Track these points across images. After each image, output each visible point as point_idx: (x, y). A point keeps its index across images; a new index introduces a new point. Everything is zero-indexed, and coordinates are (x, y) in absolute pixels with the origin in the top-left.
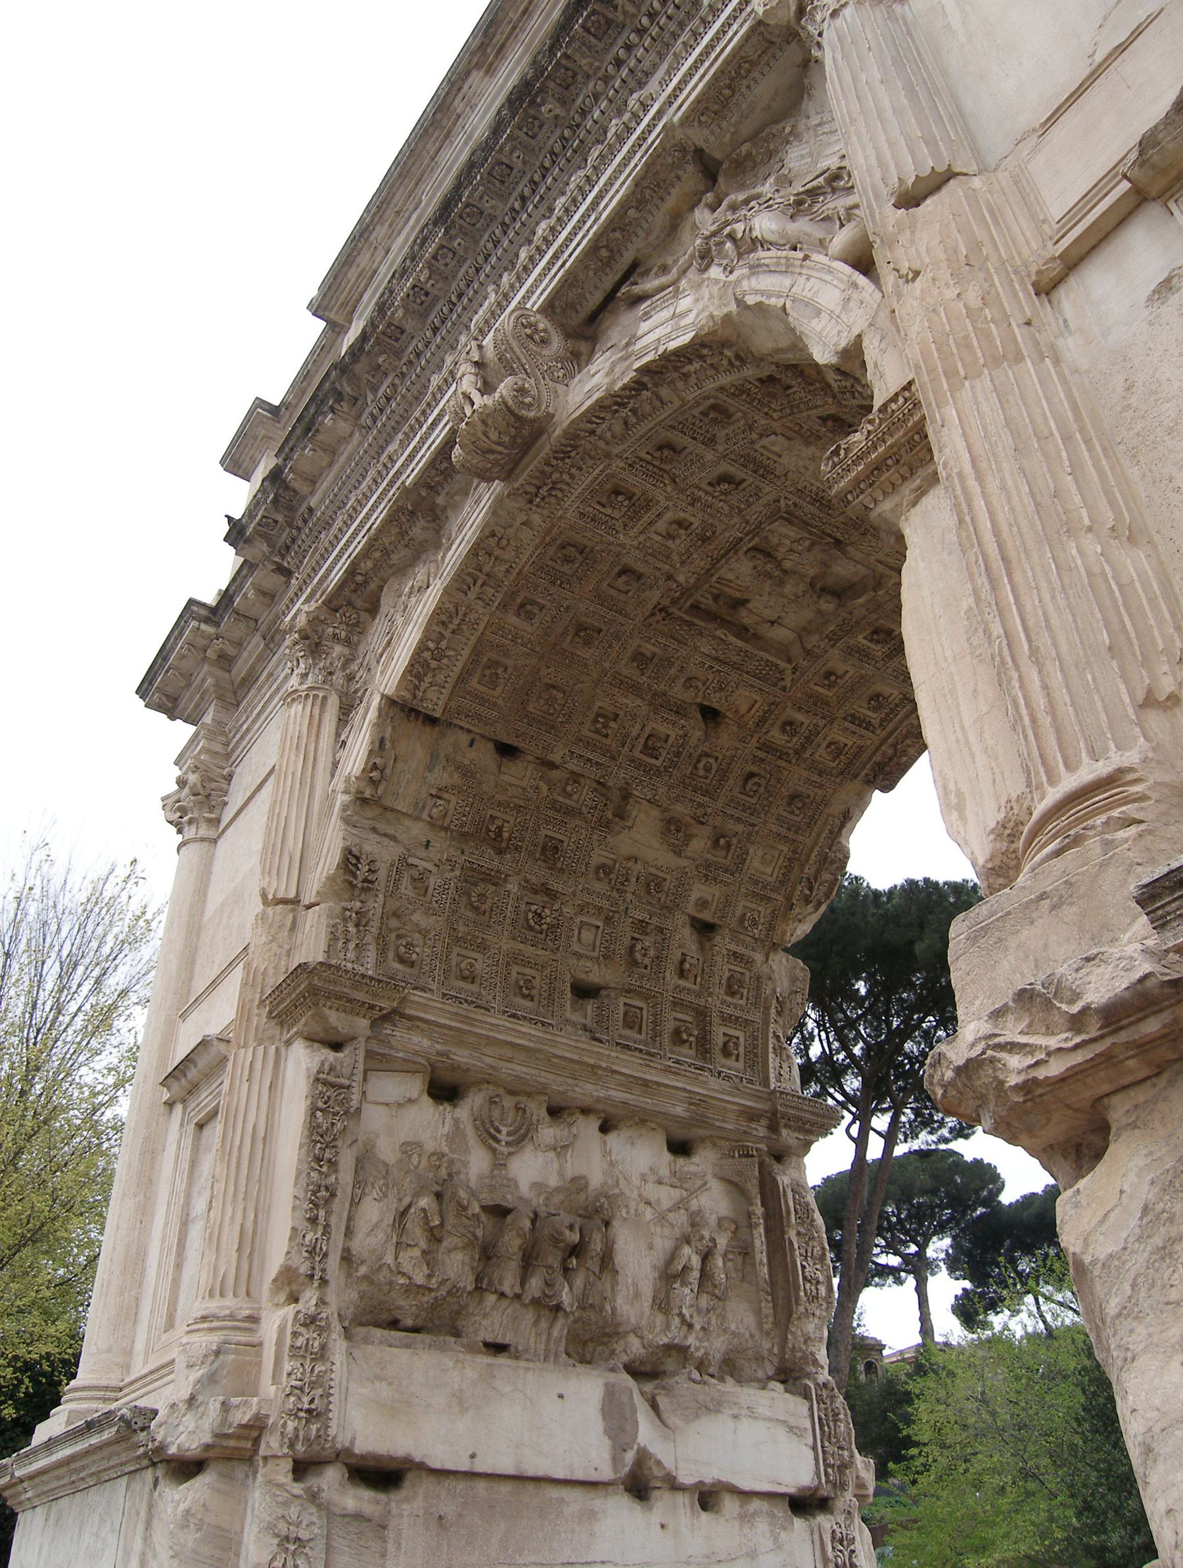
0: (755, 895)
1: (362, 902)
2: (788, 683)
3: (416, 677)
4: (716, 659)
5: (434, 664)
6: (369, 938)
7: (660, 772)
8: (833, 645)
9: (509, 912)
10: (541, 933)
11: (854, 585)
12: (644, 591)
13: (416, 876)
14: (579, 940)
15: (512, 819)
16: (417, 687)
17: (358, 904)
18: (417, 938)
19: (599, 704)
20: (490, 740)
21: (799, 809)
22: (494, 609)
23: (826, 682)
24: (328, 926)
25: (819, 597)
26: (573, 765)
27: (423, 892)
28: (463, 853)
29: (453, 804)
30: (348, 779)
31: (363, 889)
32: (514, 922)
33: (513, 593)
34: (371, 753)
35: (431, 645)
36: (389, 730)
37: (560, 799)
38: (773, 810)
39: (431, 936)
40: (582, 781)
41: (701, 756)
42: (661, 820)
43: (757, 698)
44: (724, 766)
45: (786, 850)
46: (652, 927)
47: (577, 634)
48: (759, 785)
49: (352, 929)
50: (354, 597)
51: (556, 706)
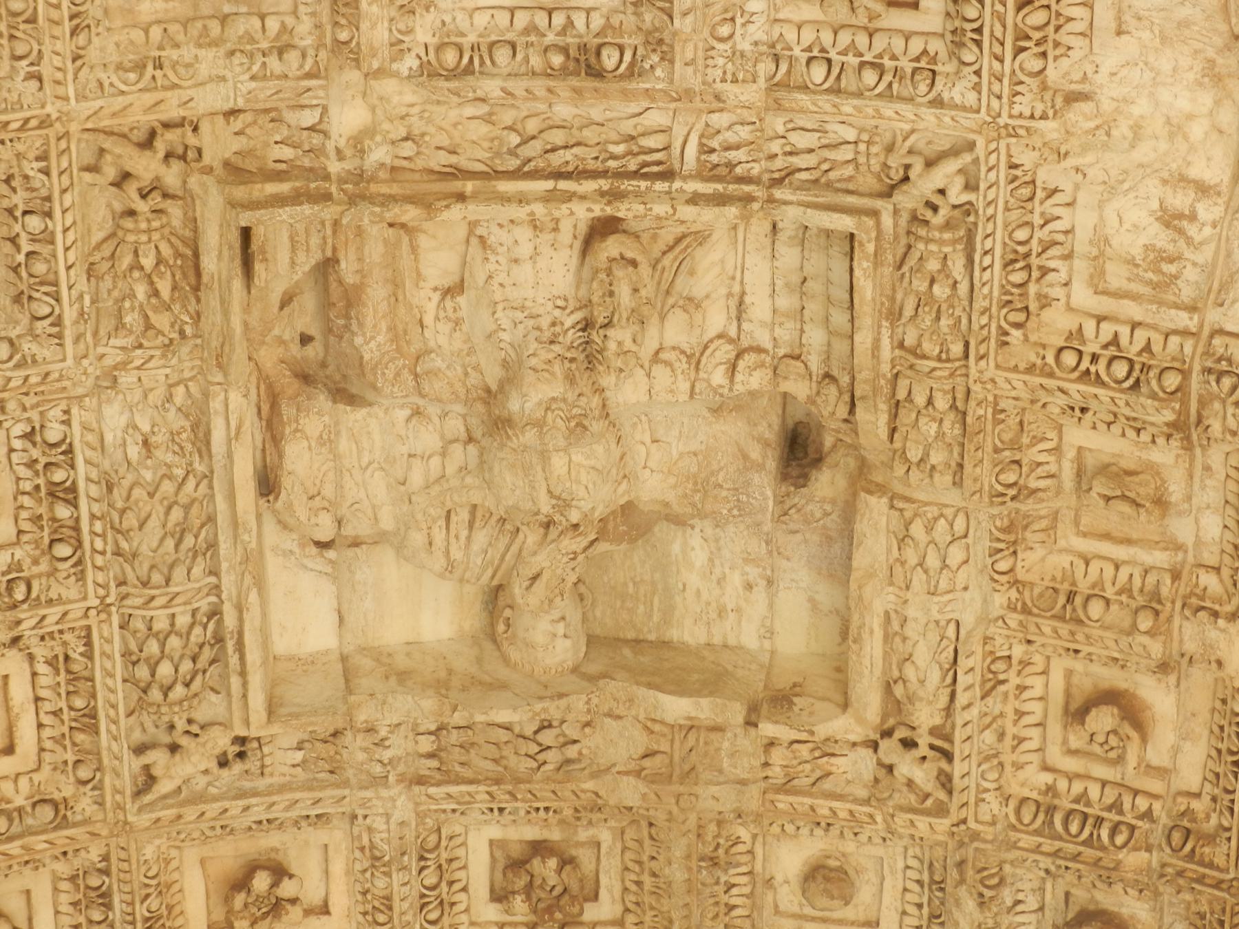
8: (421, 781)
11: (665, 644)
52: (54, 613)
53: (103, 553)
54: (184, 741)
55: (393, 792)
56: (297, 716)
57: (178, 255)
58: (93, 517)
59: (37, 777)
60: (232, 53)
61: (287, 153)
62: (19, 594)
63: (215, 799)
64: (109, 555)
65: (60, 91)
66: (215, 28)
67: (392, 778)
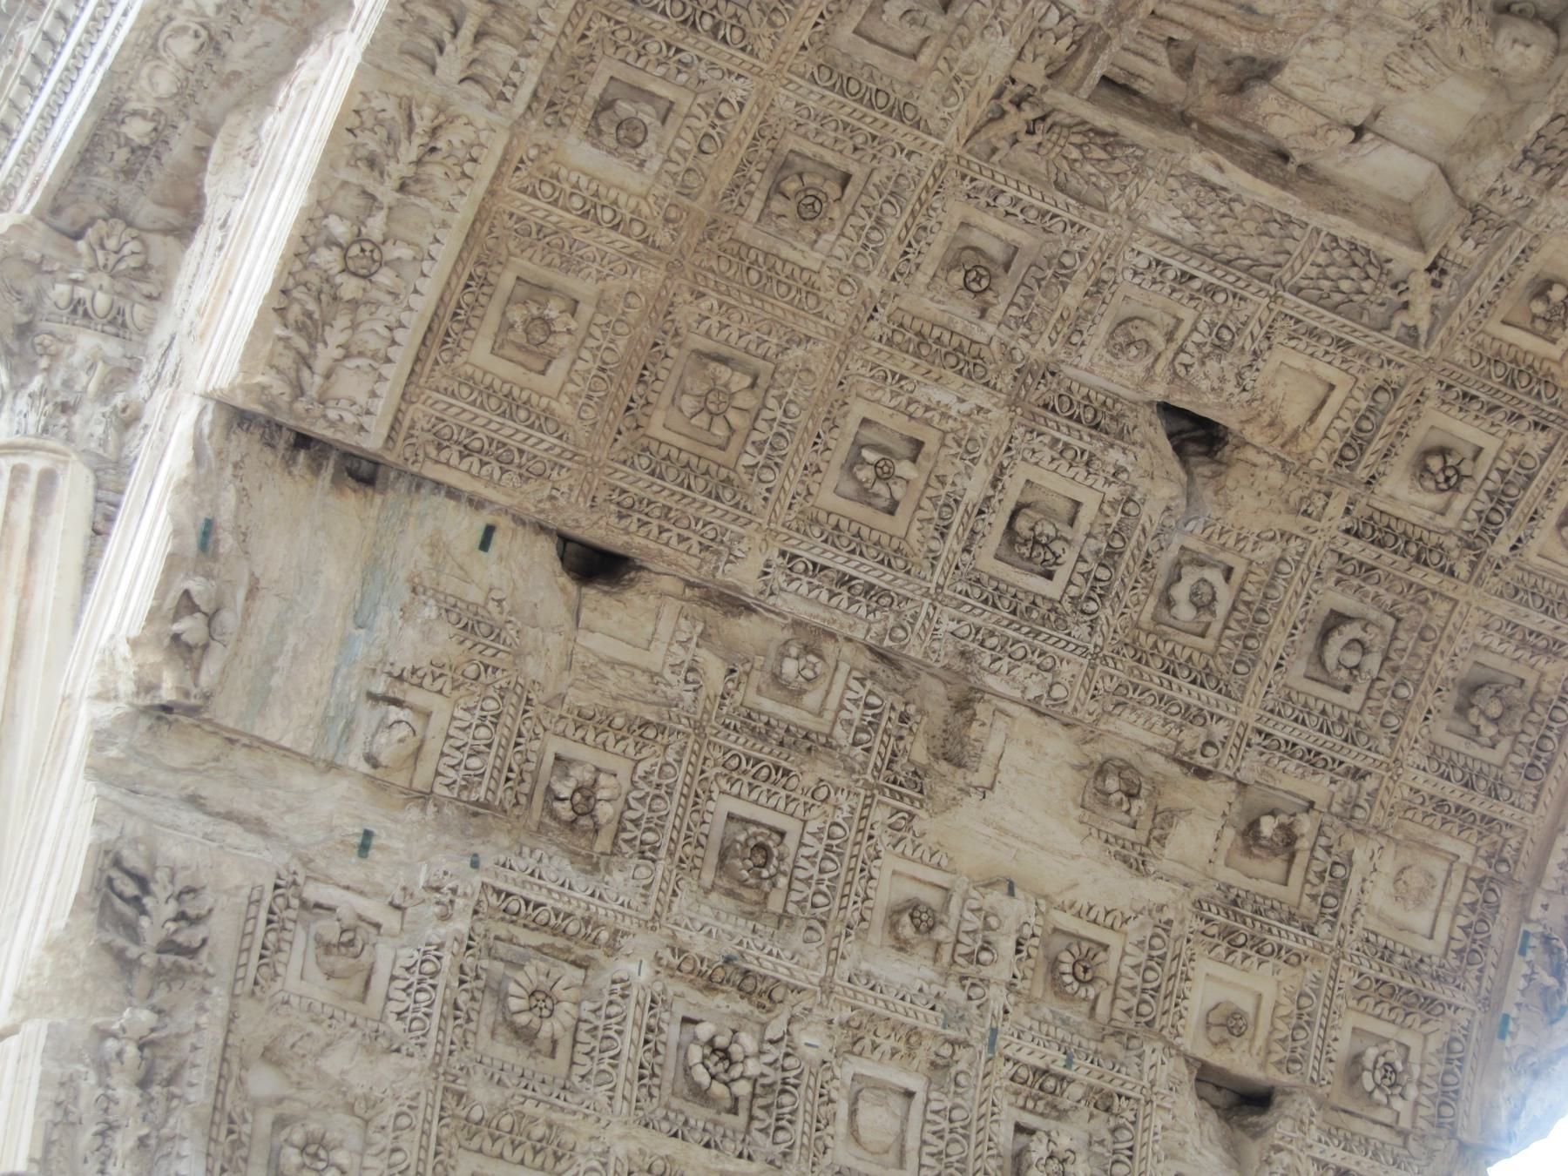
0: (1385, 992)
1: (160, 1012)
2: (1420, 315)
3: (300, 328)
4: (1199, 250)
5: (350, 288)
6: (180, 1121)
7: (1061, 617)
8: (1550, 184)
9: (628, 1043)
10: (734, 1110)
12: (965, 43)
13: (333, 936)
14: (854, 1133)
15: (623, 767)
16: (305, 361)
17: (145, 1017)
18: (341, 1126)
19: (859, 409)
20: (541, 528)
21: (1495, 721)
22: (519, 108)
23: (1539, 307)
24: (44, 1082)
25: (1494, 27)
26: (798, 601)
27: (355, 987)
28: (475, 864)
29: (439, 721)
30: (108, 662)
31: (159, 973)
32: (645, 1075)
33: (575, 61)
34: (173, 564)
35: (340, 229)
36: (230, 497)
37: (768, 705)
38: (1414, 728)
39: (385, 1119)
40: (829, 647)
41: (1178, 565)
42: (1080, 768)
43: (1332, 374)
44: (1253, 592)
45: (1466, 854)
46: (1075, 1091)
47: (777, 190)
48: (1365, 650)
49: (124, 1092)
50: (126, 193)
51: (733, 417)
52: (1254, 326)
53: (1239, 279)
54: (1404, 298)
55: (1544, 203)
56: (1436, 235)
57: (1084, 134)
58: (1210, 272)
59: (1360, 384)
60: (982, 35)
61: (1066, 41)
62: (1227, 336)
63: (1458, 302)
64: (1244, 276)
65: (929, 146)
66: (963, 31)
67: (1535, 197)
